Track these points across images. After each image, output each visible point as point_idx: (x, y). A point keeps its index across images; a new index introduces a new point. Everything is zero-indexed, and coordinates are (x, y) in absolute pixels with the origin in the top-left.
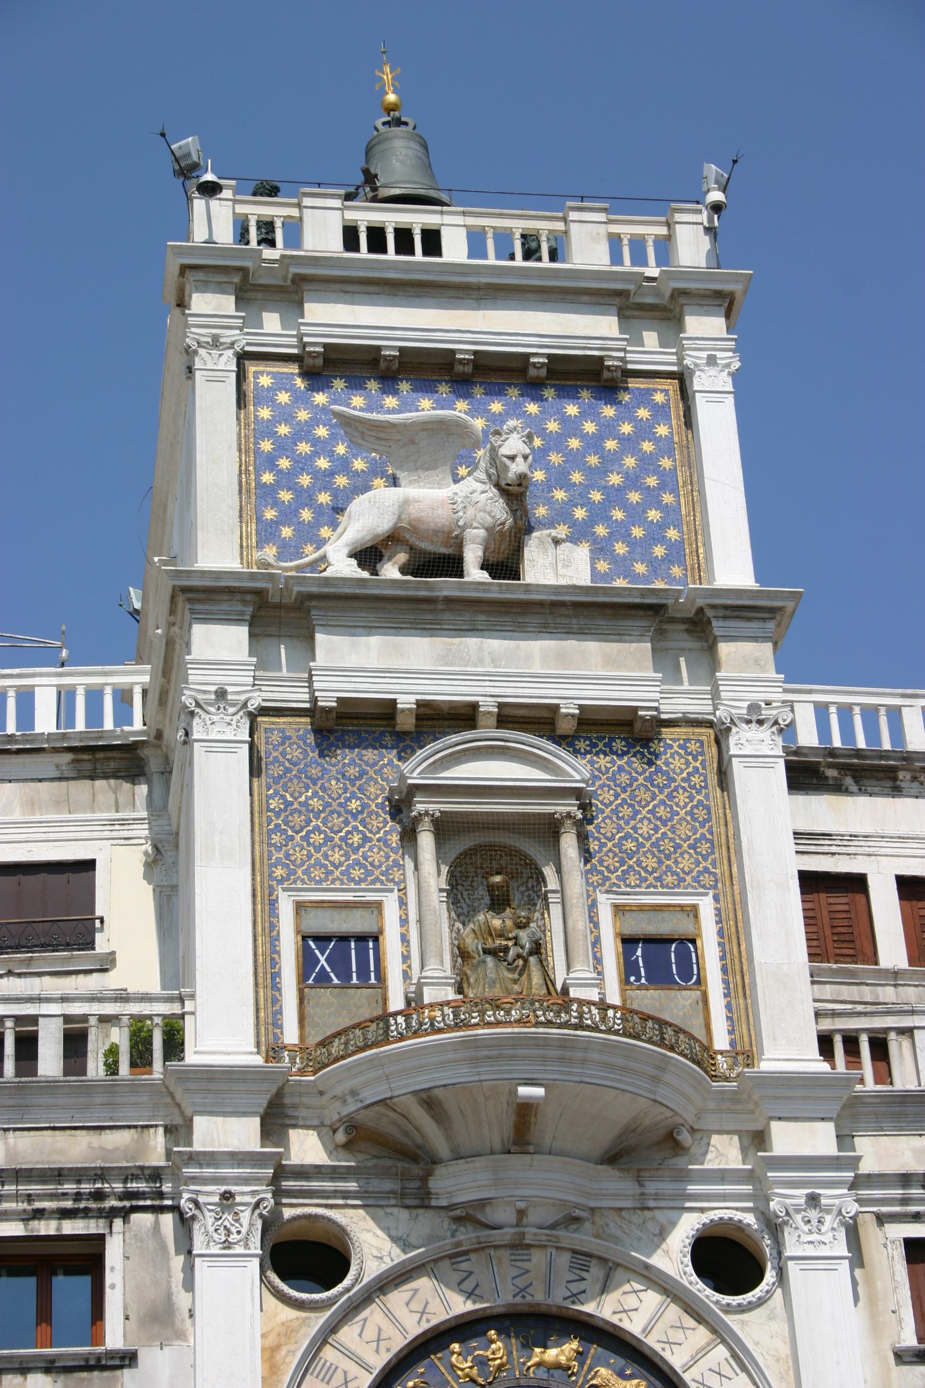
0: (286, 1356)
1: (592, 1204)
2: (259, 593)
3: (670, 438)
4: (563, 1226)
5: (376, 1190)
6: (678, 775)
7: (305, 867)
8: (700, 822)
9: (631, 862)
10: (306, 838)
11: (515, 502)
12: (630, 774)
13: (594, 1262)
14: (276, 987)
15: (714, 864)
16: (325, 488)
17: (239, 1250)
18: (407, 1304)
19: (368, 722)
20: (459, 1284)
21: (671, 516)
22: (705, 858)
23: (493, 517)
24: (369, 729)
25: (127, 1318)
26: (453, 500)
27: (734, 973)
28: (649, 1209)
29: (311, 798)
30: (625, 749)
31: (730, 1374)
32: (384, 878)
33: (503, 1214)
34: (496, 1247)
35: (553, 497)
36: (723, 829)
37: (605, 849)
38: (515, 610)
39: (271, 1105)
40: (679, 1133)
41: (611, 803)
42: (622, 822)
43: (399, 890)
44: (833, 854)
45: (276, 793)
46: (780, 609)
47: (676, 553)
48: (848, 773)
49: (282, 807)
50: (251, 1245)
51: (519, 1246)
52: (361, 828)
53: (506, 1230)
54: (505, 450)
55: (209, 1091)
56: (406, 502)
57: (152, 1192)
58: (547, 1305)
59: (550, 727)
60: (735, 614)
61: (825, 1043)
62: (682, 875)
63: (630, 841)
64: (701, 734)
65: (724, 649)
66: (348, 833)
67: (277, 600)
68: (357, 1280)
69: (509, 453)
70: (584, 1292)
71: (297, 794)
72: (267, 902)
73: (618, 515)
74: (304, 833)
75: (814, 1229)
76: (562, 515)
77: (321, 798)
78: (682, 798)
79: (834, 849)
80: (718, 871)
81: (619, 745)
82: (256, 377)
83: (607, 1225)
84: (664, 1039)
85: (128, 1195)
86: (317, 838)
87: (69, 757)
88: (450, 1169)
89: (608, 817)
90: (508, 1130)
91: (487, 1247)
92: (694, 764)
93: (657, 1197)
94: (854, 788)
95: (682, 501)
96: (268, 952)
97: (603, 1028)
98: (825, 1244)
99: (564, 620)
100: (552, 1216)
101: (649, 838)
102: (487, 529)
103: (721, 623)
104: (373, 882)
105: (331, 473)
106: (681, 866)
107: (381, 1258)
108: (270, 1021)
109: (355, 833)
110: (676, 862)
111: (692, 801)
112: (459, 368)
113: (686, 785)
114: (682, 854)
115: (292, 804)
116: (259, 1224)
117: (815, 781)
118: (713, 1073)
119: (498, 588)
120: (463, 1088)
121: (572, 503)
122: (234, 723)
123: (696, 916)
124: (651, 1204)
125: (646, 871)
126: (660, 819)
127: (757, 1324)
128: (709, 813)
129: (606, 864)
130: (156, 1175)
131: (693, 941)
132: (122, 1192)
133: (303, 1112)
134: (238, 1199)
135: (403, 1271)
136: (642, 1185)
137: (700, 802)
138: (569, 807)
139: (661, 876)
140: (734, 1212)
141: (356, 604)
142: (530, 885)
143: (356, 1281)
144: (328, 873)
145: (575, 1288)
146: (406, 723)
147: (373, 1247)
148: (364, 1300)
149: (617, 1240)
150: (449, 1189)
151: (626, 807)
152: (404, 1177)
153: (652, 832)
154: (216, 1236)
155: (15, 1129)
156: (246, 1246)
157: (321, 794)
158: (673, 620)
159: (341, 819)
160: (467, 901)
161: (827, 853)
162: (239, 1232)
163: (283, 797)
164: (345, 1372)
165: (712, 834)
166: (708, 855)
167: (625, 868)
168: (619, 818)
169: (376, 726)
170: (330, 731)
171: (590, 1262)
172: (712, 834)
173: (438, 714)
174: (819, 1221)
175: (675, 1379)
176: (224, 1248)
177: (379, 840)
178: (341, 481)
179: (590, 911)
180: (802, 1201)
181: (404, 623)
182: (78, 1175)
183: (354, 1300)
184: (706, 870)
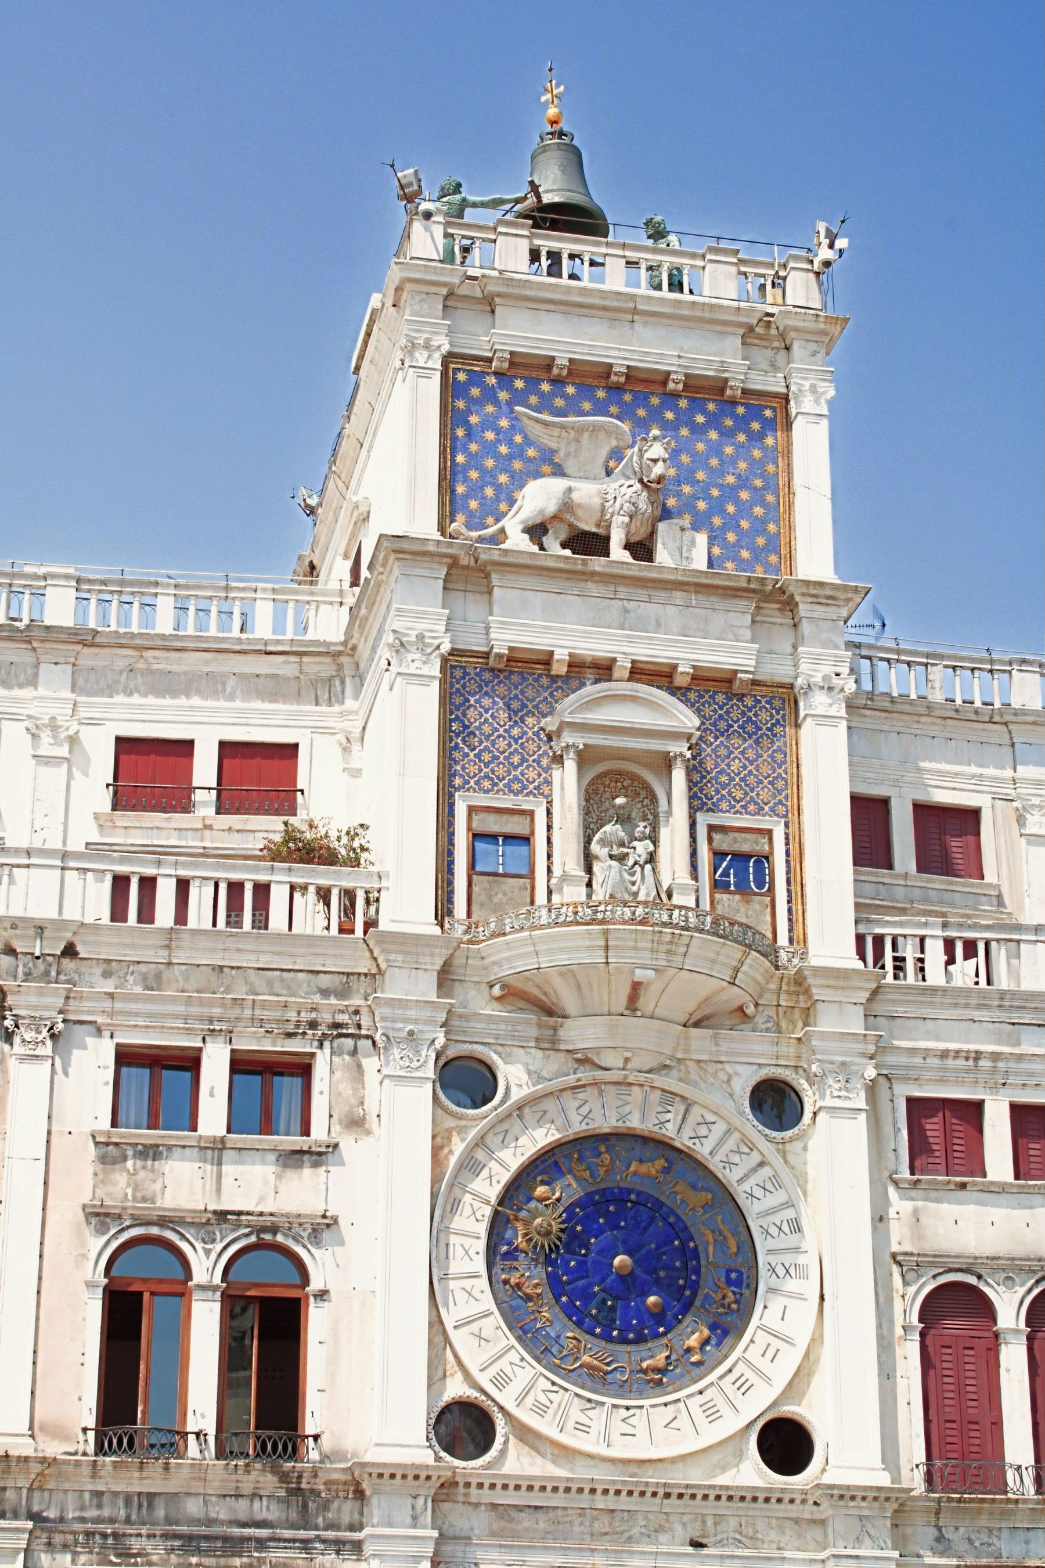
13: (678, 1099)
14: (451, 871)
16: (506, 471)
22: (780, 792)
25: (331, 1116)
26: (609, 497)
33: (610, 1059)
34: (606, 1083)
39: (445, 964)
45: (457, 718)
56: (570, 490)
76: (688, 506)
81: (720, 698)
82: (454, 374)
85: (336, 1026)
86: (486, 757)
100: (651, 1063)
101: (739, 774)
104: (527, 795)
110: (758, 794)
112: (614, 378)
116: (433, 1056)
124: (723, 1059)
126: (747, 759)
131: (767, 858)
136: (717, 1045)
138: (681, 748)
141: (527, 571)
143: (503, 1102)
144: (495, 784)
146: (559, 669)
147: (515, 1077)
163: (463, 722)
168: (717, 756)
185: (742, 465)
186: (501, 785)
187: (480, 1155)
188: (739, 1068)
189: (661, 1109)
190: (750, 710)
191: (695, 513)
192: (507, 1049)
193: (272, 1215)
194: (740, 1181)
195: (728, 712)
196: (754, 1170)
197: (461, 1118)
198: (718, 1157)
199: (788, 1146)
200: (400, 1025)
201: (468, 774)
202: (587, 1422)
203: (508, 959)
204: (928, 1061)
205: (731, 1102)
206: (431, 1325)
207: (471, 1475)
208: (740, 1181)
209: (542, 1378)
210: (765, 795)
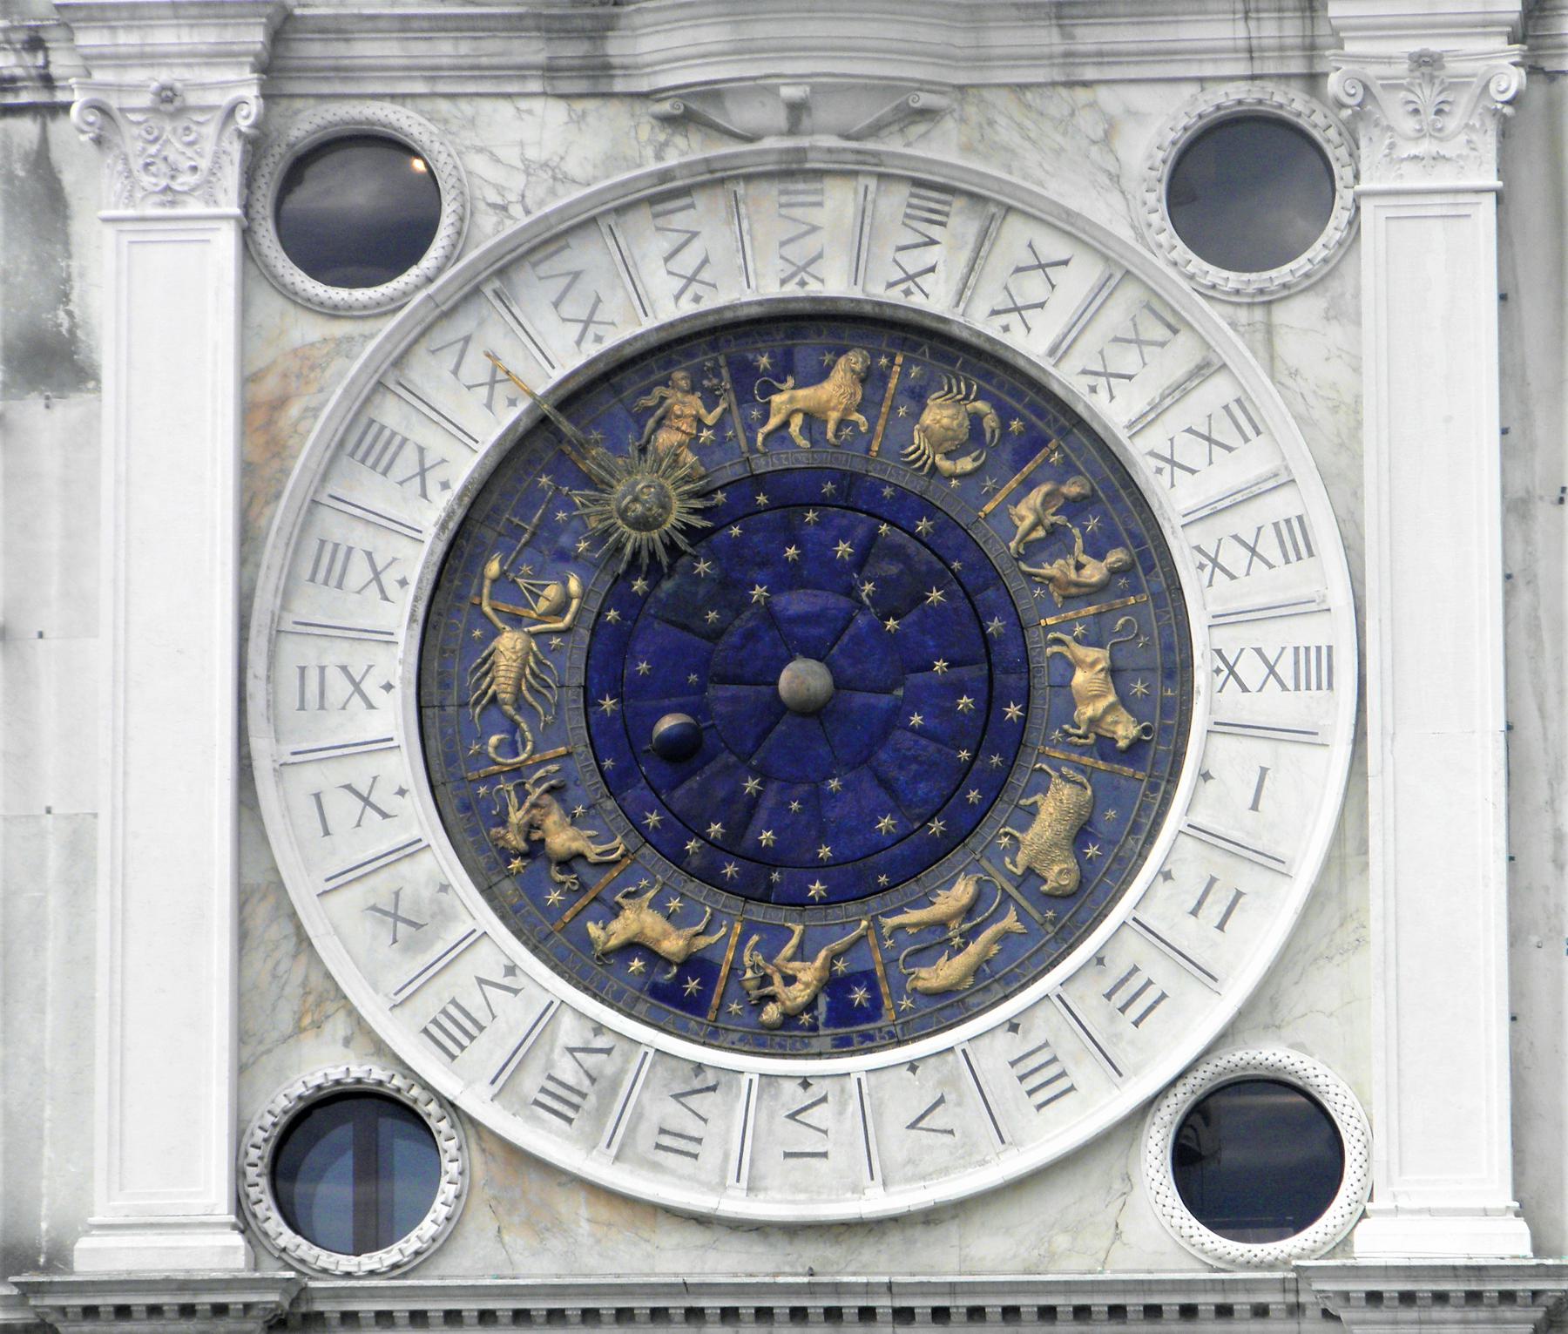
0: (302, 418)
1: (961, 78)
4: (895, 128)
13: (959, 203)
17: (195, 207)
18: (556, 305)
20: (667, 260)
28: (1086, 84)
31: (1233, 439)
50: (221, 197)
51: (794, 171)
53: (769, 143)
57: (30, 78)
58: (852, 300)
68: (448, 258)
70: (932, 269)
83: (991, 123)
91: (730, 178)
100: (866, 113)
107: (504, 208)
116: (235, 149)
124: (1090, 74)
135: (547, 235)
136: (1067, 35)
140: (1270, 86)
145: (914, 261)
148: (466, 299)
154: (147, 180)
156: (212, 200)
164: (421, 450)
171: (950, 204)
174: (1439, 112)
176: (163, 204)
180: (1402, 68)
187: (391, 414)
188: (1139, 97)
189: (910, 238)
192: (465, 107)
194: (1140, 425)
196: (1179, 390)
197: (334, 312)
199: (1281, 314)
200: (136, 76)
202: (693, 1127)
205: (1115, 199)
206: (244, 898)
207: (353, 1293)
208: (1140, 425)
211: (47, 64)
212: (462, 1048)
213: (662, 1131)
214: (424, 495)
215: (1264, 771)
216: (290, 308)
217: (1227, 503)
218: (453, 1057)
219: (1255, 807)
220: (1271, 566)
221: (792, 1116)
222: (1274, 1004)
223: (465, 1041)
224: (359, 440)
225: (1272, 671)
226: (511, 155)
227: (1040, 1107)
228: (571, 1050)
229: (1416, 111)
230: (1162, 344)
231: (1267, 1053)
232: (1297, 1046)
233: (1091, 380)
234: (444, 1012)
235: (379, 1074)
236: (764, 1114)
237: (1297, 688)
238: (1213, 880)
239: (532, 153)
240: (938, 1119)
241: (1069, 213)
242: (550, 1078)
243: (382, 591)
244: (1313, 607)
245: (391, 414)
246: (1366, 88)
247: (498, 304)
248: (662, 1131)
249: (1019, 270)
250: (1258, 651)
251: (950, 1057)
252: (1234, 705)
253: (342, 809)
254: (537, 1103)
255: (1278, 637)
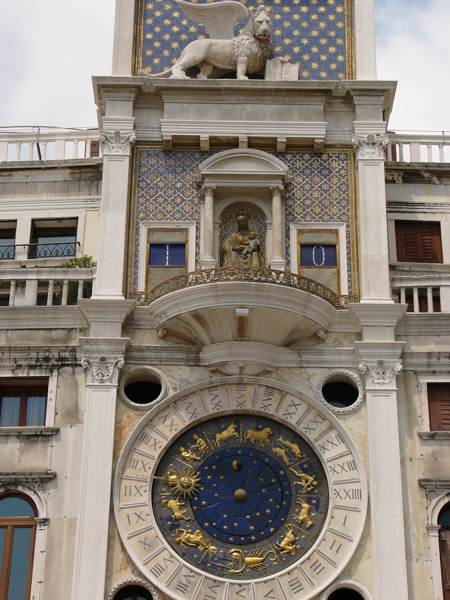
2: (139, 88)
3: (343, 13)
5: (175, 357)
6: (334, 170)
7: (154, 213)
8: (343, 191)
9: (308, 210)
10: (155, 200)
11: (263, 44)
12: (311, 169)
13: (276, 391)
15: (348, 211)
16: (176, 41)
18: (186, 409)
19: (187, 147)
21: (341, 50)
22: (344, 208)
23: (251, 51)
24: (188, 150)
25: (56, 414)
27: (354, 261)
28: (304, 368)
29: (159, 182)
30: (309, 158)
32: (190, 218)
34: (230, 384)
35: (284, 42)
36: (354, 194)
37: (296, 204)
38: (259, 94)
40: (319, 333)
41: (301, 183)
42: (305, 192)
43: (197, 223)
44: (425, 213)
46: (386, 90)
47: (342, 67)
48: (434, 175)
49: (145, 186)
50: (113, 382)
51: (240, 384)
52: (181, 195)
54: (258, 19)
55: (98, 312)
56: (210, 46)
57: (72, 358)
59: (274, 148)
60: (365, 93)
61: (396, 292)
62: (332, 216)
63: (308, 200)
64: (346, 151)
65: (358, 110)
66: (175, 197)
67: (147, 91)
69: (259, 20)
70: (270, 405)
71: (152, 180)
72: (135, 229)
73: (315, 50)
74: (154, 198)
75: (381, 377)
76: (287, 50)
77: (164, 182)
78: (335, 180)
79: (425, 210)
80: (350, 214)
81: (306, 157)
84: (309, 288)
85: (61, 359)
86: (161, 200)
87: (69, 171)
88: (209, 348)
89: (298, 189)
90: (235, 330)
92: (342, 165)
93: (308, 362)
94: (437, 182)
95: (346, 43)
96: (134, 251)
97: (278, 282)
98: (385, 384)
99: (282, 98)
100: (257, 370)
101: (318, 199)
102: (248, 57)
103: (358, 98)
104: (185, 220)
105: (179, 33)
106: (332, 212)
107: (176, 389)
108: (132, 282)
109: (178, 198)
110: (330, 210)
111: (340, 182)
113: (337, 174)
114: (333, 206)
115: (150, 184)
117: (418, 179)
118: (337, 305)
119: (249, 83)
120: (211, 309)
121: (293, 45)
122: (123, 147)
123: (337, 235)
124: (305, 365)
125: (315, 214)
126: (324, 190)
127: (351, 422)
128: (348, 187)
129: (296, 211)
130: (73, 350)
132: (58, 358)
133: (144, 323)
134: (108, 361)
137: (344, 182)
139: (322, 216)
142: (260, 221)
143: (163, 398)
144: (165, 215)
145: (266, 403)
148: (166, 407)
149: (288, 382)
150: (208, 358)
151: (307, 185)
152: (188, 351)
153: (319, 196)
154: (97, 377)
155: (12, 330)
156: (111, 382)
157: (164, 180)
158: (336, 97)
159: (172, 191)
160: (232, 229)
161: (422, 212)
162: (108, 375)
163: (146, 182)
164: (155, 439)
165: (348, 197)
166: (346, 206)
167: (305, 212)
168: (304, 190)
169: (192, 149)
170: (170, 151)
172: (348, 197)
173: (222, 143)
174: (383, 374)
175: (311, 445)
176: (101, 383)
177: (189, 201)
178: (184, 37)
179: (286, 233)
181: (206, 101)
182: (38, 349)
183: (161, 407)
184: (344, 213)
185: (322, 25)
186: (169, 216)
187: (148, 431)
188: (316, 371)
190: (325, 162)
191: (293, 54)
192: (167, 367)
193: (14, 474)
194: (316, 440)
195: (311, 164)
196: (325, 433)
197: (136, 409)
198: (302, 425)
201: (148, 211)
203: (164, 313)
204: (441, 360)
205: (311, 391)
208: (316, 440)
209: (184, 569)
210: (334, 211)
211: (76, 355)
212: (159, 575)
213: (206, 596)
214: (155, 449)
215: (346, 517)
216: (127, 408)
217: (336, 457)
218: (157, 577)
219: (344, 525)
220: (347, 471)
221: (237, 593)
222: (350, 570)
223: (160, 573)
224: (140, 436)
225: (347, 494)
226: (178, 377)
227: (295, 593)
228: (185, 576)
229: (378, 373)
230: (321, 423)
231: (349, 582)
232: (355, 580)
233: (306, 430)
234: (155, 566)
235: (140, 580)
236: (230, 593)
237: (353, 498)
238: (335, 541)
239: (182, 377)
240: (272, 595)
241: (300, 394)
242: (180, 582)
243: (145, 470)
244: (356, 480)
245: (148, 431)
246: (368, 369)
247: (174, 409)
248: (206, 596)
249: (289, 406)
250: (344, 490)
251: (274, 581)
252: (340, 502)
253: (134, 518)
254: (176, 588)
255: (348, 487)
